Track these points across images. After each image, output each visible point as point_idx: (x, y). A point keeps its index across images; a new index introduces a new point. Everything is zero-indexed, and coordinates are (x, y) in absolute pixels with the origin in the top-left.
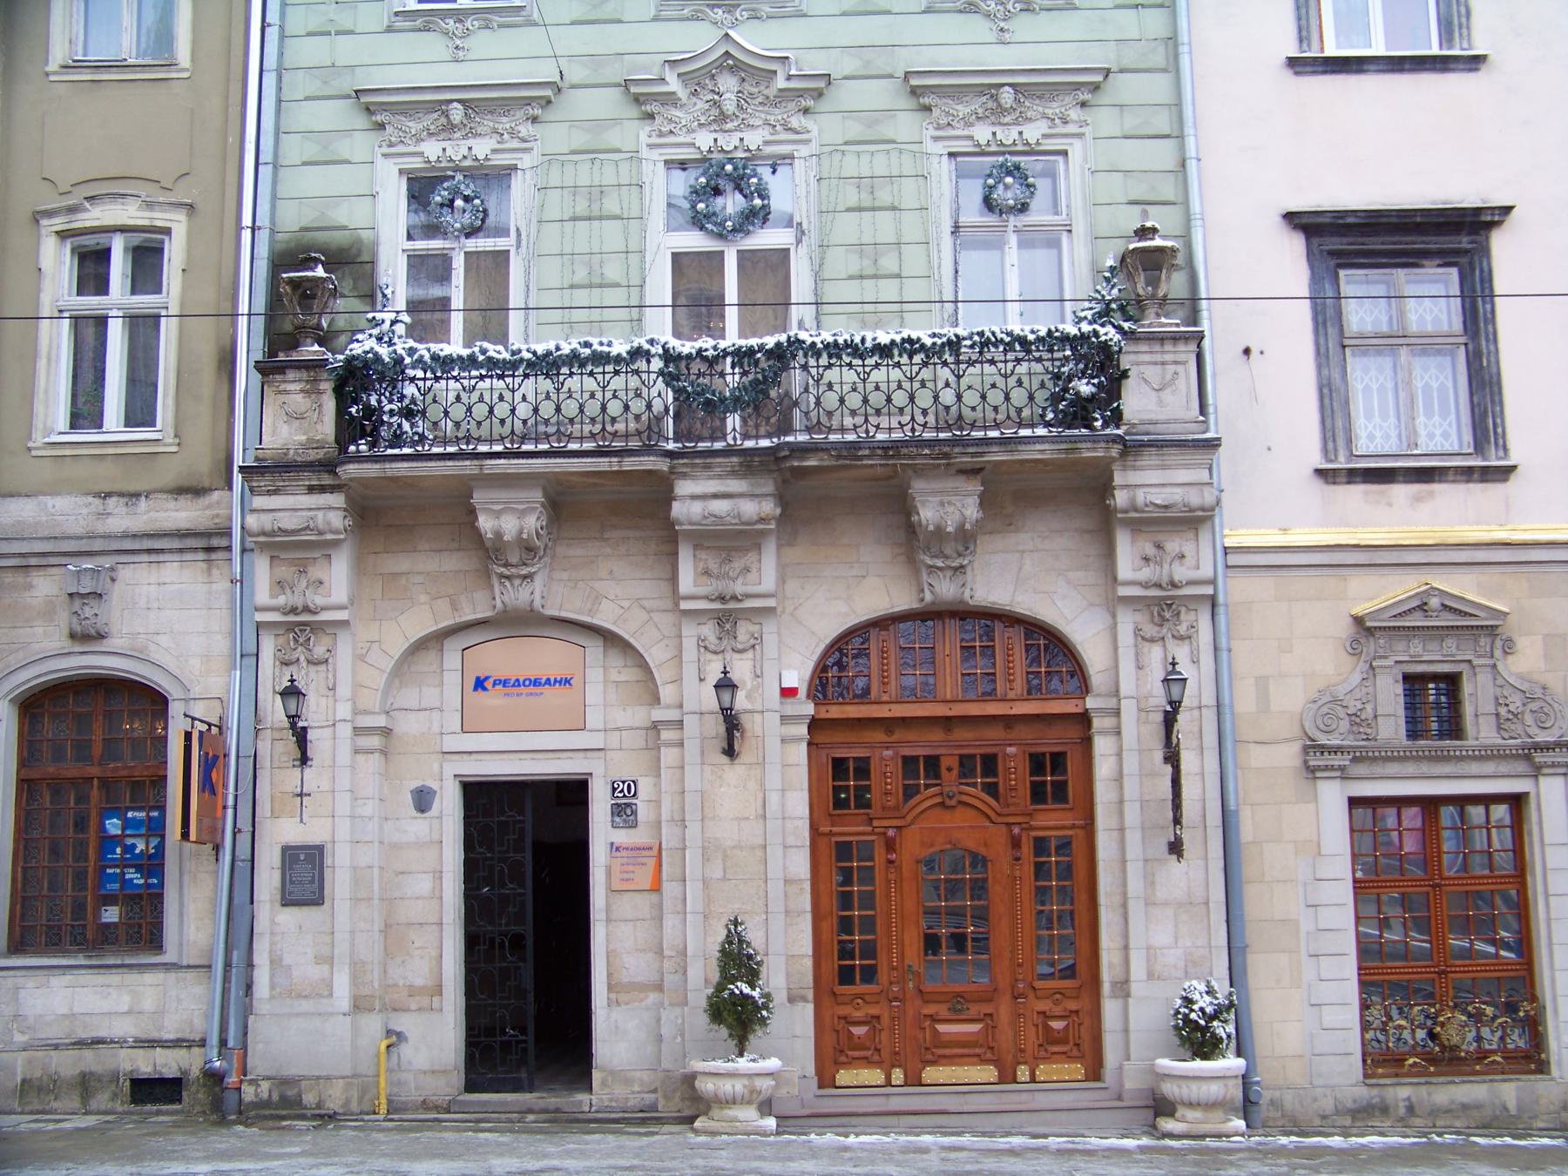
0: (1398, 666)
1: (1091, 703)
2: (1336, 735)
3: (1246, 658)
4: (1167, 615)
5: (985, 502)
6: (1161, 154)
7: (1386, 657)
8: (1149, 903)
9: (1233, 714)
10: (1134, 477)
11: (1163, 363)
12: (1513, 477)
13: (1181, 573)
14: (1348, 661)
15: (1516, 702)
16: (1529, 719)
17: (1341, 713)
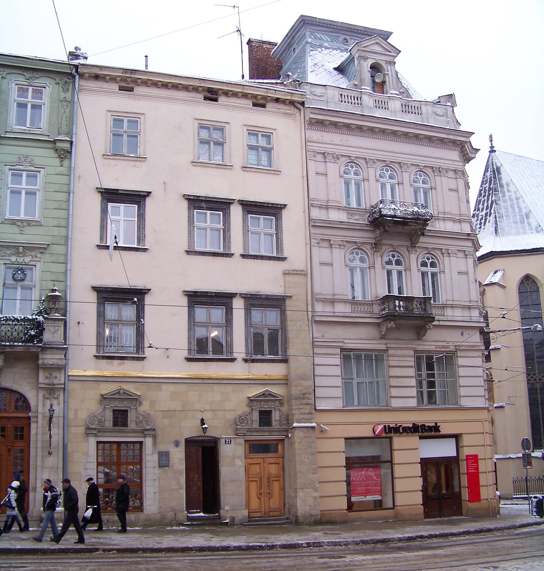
0: (112, 408)
1: (30, 414)
2: (94, 425)
3: (73, 404)
4: (52, 392)
5: (5, 360)
6: (60, 268)
7: (108, 405)
8: (43, 467)
9: (67, 419)
10: (45, 356)
11: (55, 326)
12: (145, 359)
13: (56, 381)
14: (99, 406)
15: (141, 418)
16: (144, 423)
17: (96, 419)
